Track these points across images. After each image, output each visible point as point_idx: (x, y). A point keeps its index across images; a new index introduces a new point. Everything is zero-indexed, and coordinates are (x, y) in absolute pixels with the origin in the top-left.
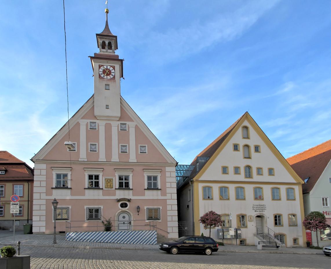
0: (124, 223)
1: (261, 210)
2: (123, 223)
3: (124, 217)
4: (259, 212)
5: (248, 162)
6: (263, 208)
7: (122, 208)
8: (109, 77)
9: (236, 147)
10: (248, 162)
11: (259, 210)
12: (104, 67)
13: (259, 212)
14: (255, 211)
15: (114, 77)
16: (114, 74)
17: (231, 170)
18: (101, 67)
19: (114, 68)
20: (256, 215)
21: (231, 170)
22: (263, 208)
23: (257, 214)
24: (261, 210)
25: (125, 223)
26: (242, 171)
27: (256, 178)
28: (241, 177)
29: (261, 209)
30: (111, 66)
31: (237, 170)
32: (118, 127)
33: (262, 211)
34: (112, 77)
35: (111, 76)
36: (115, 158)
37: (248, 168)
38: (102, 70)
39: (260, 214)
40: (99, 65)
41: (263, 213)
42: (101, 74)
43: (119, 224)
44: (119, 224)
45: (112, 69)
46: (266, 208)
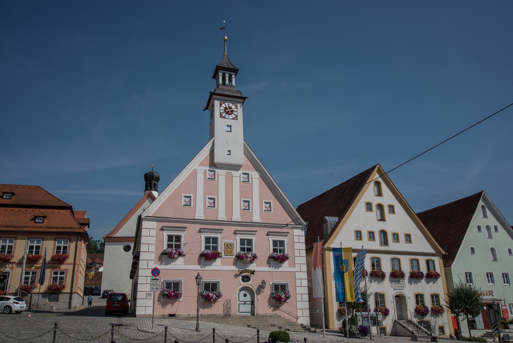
0: (245, 304)
1: (401, 288)
2: (243, 303)
3: (245, 295)
4: (398, 291)
5: (382, 226)
6: (402, 285)
7: (244, 282)
8: (231, 117)
9: (369, 206)
10: (382, 226)
11: (398, 288)
12: (225, 105)
13: (398, 291)
14: (394, 289)
15: (237, 117)
16: (236, 113)
17: (365, 235)
18: (222, 104)
19: (236, 107)
20: (396, 295)
21: (365, 235)
22: (402, 285)
23: (396, 293)
24: (401, 288)
25: (247, 303)
26: (377, 236)
27: (393, 246)
28: (376, 245)
29: (400, 287)
30: (233, 104)
31: (371, 235)
32: (240, 177)
33: (402, 289)
34: (234, 116)
35: (233, 115)
36: (237, 217)
37: (384, 233)
38: (223, 108)
39: (399, 292)
40: (220, 102)
41: (403, 291)
42: (222, 113)
43: (239, 304)
44: (239, 304)
45: (235, 107)
46: (405, 286)
